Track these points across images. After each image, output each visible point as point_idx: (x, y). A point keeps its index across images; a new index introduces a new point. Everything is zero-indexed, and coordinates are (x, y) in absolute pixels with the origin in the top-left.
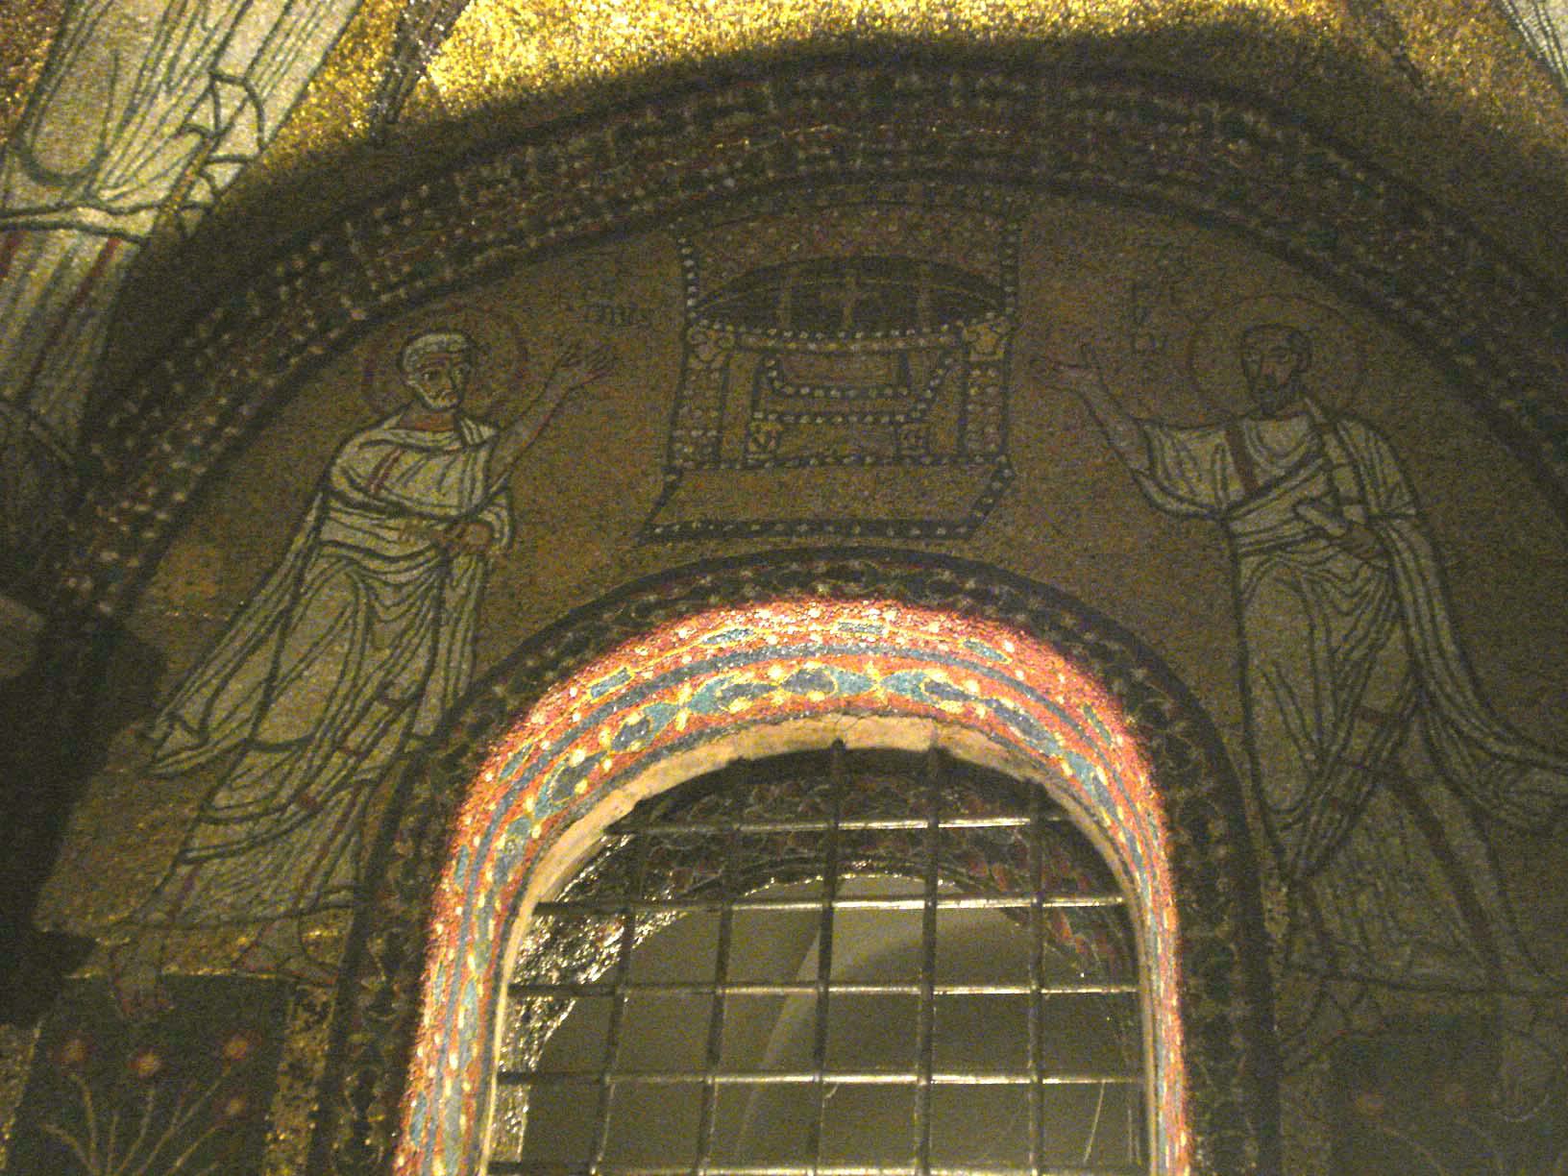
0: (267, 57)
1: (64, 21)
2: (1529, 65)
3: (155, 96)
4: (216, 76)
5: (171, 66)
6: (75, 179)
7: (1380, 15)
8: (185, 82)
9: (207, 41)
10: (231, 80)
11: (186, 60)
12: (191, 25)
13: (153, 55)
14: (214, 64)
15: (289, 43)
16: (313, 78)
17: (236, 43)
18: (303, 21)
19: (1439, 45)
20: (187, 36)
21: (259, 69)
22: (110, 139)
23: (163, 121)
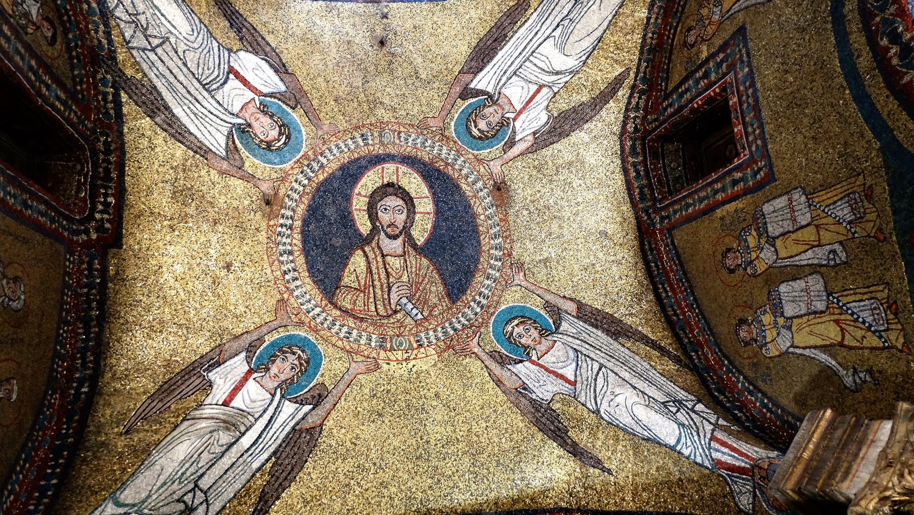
0: (214, 488)
1: (145, 460)
2: (644, 442)
3: (174, 482)
4: (196, 486)
5: (183, 474)
6: (134, 505)
7: (591, 458)
8: (186, 482)
9: (197, 471)
10: (201, 490)
11: (188, 474)
12: (193, 463)
13: (177, 469)
14: (197, 481)
15: (224, 485)
16: (229, 502)
17: (206, 476)
18: (230, 479)
19: (613, 457)
20: (192, 465)
21: (211, 490)
22: (153, 492)
23: (174, 493)
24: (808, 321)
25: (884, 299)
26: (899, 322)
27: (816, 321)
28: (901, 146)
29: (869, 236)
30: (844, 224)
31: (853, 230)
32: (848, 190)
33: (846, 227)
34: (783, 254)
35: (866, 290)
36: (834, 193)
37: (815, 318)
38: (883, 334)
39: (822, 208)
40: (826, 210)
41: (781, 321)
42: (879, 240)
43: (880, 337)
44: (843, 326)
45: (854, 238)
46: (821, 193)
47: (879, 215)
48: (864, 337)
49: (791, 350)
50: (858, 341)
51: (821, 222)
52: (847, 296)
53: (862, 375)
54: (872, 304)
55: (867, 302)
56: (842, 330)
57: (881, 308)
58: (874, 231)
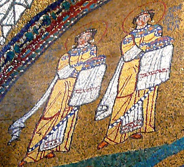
24: (69, 91)
25: (59, 149)
26: (41, 159)
27: (66, 98)
28: (160, 161)
29: (106, 136)
30: (123, 117)
31: (115, 124)
32: (146, 120)
33: (120, 119)
34: (126, 66)
35: (70, 135)
36: (149, 108)
37: (68, 96)
38: (38, 148)
39: (143, 99)
40: (140, 102)
41: (79, 68)
42: (99, 144)
43: (36, 146)
44: (54, 119)
45: (109, 125)
46: (155, 97)
47: (117, 144)
48: (41, 134)
49: (56, 78)
50: (40, 130)
51: (133, 98)
52: (72, 121)
53: (17, 134)
54: (59, 139)
55: (62, 136)
56: (51, 118)
57: (54, 147)
58: (108, 140)
